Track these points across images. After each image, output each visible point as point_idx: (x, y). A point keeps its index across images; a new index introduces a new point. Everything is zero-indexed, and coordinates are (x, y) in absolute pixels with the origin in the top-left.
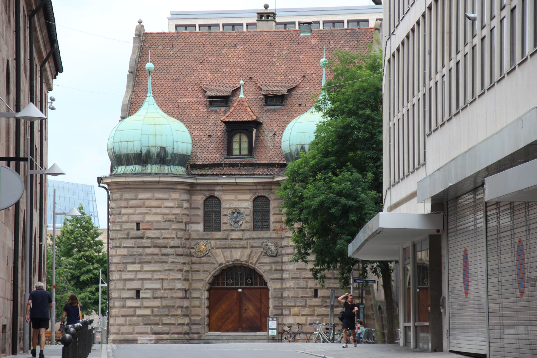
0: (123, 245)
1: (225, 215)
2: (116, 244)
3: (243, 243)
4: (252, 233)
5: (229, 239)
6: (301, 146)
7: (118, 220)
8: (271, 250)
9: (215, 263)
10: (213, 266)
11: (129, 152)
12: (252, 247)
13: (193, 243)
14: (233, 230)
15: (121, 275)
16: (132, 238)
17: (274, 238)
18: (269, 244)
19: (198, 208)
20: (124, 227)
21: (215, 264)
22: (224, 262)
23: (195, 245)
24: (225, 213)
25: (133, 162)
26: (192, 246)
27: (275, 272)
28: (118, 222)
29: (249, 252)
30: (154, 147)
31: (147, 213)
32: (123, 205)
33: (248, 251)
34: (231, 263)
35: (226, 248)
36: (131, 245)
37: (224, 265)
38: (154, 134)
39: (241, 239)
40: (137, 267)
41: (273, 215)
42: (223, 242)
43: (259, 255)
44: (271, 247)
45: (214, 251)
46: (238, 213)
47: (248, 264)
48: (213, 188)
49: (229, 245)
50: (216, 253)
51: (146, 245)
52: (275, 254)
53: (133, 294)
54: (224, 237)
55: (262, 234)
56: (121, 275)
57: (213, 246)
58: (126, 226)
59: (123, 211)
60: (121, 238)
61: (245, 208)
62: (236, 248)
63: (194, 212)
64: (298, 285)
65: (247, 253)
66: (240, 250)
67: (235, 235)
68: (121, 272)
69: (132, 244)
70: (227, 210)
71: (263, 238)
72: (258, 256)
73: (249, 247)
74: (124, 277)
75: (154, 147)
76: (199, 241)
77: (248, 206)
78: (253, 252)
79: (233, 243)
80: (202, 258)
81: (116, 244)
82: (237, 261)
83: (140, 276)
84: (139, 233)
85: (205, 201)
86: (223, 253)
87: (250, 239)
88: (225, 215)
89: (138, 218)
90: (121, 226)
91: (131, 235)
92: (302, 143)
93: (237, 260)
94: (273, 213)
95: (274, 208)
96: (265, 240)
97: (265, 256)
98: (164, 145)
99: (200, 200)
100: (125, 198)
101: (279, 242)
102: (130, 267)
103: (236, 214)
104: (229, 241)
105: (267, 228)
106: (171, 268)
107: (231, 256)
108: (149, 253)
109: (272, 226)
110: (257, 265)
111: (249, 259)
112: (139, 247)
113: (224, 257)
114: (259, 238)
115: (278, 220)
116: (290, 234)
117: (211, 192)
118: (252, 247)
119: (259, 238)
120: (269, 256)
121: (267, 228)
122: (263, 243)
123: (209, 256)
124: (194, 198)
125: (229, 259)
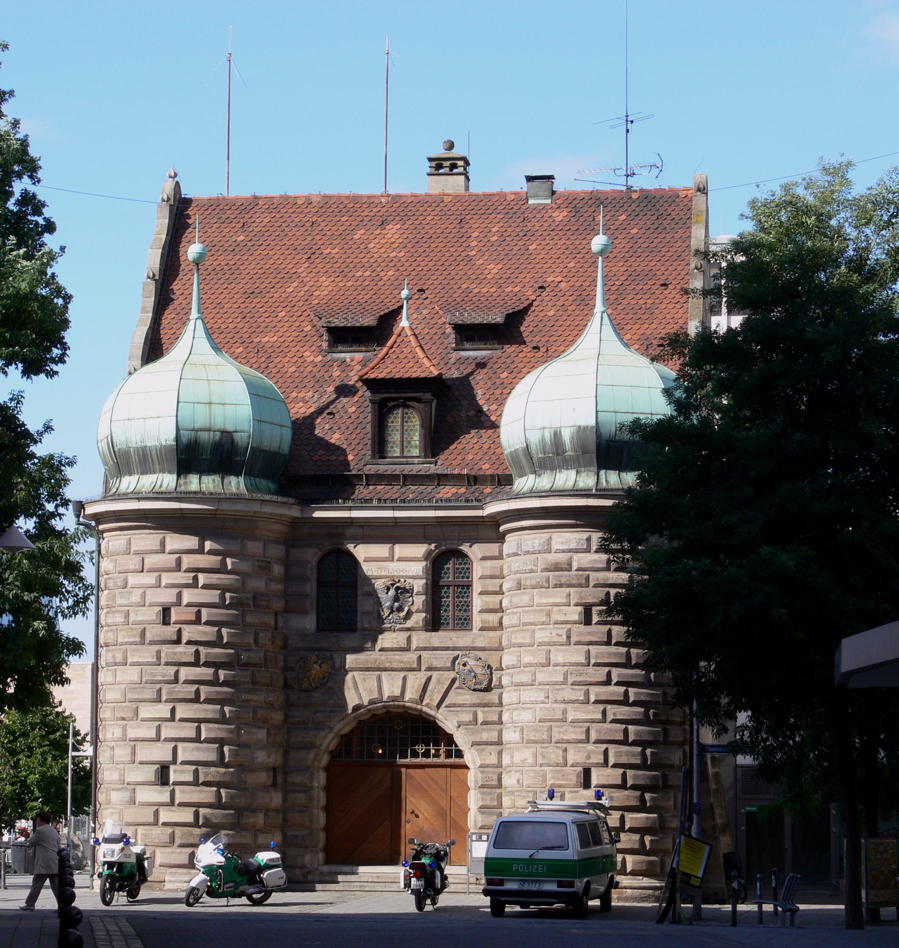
2: (114, 656)
4: (431, 637)
15: (124, 729)
16: (152, 643)
18: (472, 662)
25: (157, 467)
27: (484, 727)
29: (424, 681)
31: (187, 586)
33: (422, 676)
35: (368, 669)
36: (149, 660)
38: (208, 401)
40: (163, 710)
46: (397, 589)
49: (375, 662)
52: (483, 686)
53: (150, 773)
55: (454, 639)
56: (124, 729)
61: (414, 578)
62: (393, 670)
64: (544, 757)
68: (125, 722)
71: (454, 649)
73: (423, 668)
74: (132, 733)
75: (205, 430)
78: (433, 680)
81: (114, 656)
83: (168, 731)
84: (170, 631)
85: (320, 562)
96: (460, 653)
97: (460, 691)
98: (230, 428)
100: (137, 549)
102: (147, 711)
105: (464, 623)
109: (477, 620)
110: (441, 710)
112: (167, 664)
114: (447, 649)
116: (523, 638)
118: (430, 669)
119: (447, 649)
121: (464, 623)
122: (456, 659)
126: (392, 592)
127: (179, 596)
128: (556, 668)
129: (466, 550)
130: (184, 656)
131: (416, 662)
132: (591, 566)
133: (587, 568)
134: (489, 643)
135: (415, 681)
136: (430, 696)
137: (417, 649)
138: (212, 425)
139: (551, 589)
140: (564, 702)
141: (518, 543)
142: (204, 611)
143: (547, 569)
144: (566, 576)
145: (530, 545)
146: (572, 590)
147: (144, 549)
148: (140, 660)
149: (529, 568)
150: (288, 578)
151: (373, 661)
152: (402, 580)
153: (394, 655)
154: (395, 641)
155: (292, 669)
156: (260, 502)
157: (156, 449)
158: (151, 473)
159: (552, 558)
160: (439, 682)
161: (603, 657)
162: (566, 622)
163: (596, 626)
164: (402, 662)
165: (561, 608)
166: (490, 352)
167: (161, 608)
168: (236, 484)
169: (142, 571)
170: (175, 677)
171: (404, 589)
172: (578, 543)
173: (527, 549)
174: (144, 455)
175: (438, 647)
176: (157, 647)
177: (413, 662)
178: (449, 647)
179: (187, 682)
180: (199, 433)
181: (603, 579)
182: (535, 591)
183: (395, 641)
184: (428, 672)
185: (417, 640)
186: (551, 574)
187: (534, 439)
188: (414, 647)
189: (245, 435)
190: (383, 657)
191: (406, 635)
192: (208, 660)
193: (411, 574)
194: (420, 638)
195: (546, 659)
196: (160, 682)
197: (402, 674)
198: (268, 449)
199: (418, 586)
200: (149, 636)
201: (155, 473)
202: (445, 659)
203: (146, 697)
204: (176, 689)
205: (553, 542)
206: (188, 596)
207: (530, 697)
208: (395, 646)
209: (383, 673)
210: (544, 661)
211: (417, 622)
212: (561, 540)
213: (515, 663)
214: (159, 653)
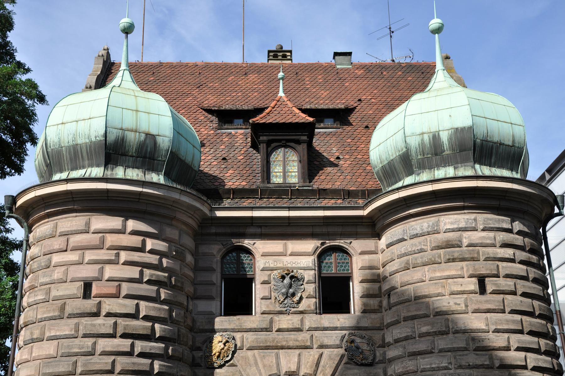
0: (47, 334)
2: (32, 333)
3: (304, 337)
4: (321, 318)
5: (275, 329)
6: (431, 135)
7: (42, 280)
8: (362, 353)
11: (79, 141)
12: (321, 347)
14: (281, 313)
16: (71, 316)
20: (54, 293)
25: (86, 162)
28: (42, 284)
29: (317, 357)
30: (132, 131)
31: (109, 262)
32: (56, 247)
33: (314, 354)
35: (267, 348)
36: (67, 333)
38: (135, 109)
42: (263, 336)
44: (360, 345)
46: (292, 277)
48: (242, 230)
49: (273, 341)
51: (103, 331)
54: (264, 326)
55: (341, 320)
58: (57, 291)
59: (56, 258)
60: (45, 319)
61: (305, 269)
62: (289, 348)
63: (203, 277)
67: (285, 321)
69: (71, 331)
73: (315, 346)
75: (132, 131)
78: (324, 356)
79: (282, 338)
81: (32, 333)
84: (89, 305)
87: (316, 329)
89: (88, 272)
90: (49, 292)
91: (68, 310)
92: (434, 129)
98: (154, 131)
99: (215, 253)
100: (63, 230)
101: (377, 336)
103: (287, 280)
104: (274, 335)
108: (108, 349)
112: (85, 336)
114: (335, 329)
118: (321, 347)
119: (335, 329)
120: (357, 364)
124: (204, 249)
126: (287, 280)
127: (101, 271)
128: (456, 335)
129: (347, 247)
130: (103, 327)
131: (309, 340)
132: (480, 242)
133: (477, 244)
134: (372, 323)
135: (310, 356)
136: (322, 370)
137: (310, 330)
138: (138, 127)
139: (443, 265)
140: (469, 367)
141: (404, 230)
142: (124, 285)
143: (438, 246)
144: (458, 251)
145: (419, 229)
146: (464, 264)
147: (69, 229)
148: (58, 334)
150: (196, 269)
152: (295, 271)
153: (290, 335)
154: (290, 322)
156: (180, 191)
157: (87, 148)
158: (80, 169)
159: (442, 237)
160: (330, 358)
161: (502, 324)
162: (463, 293)
163: (491, 295)
164: (297, 341)
165: (455, 280)
166: (335, 129)
167: (82, 283)
168: (157, 178)
169: (66, 251)
170: (93, 349)
171: (296, 277)
172: (466, 223)
173: (415, 232)
174: (75, 153)
175: (328, 328)
176: (76, 320)
177: (307, 341)
178: (337, 327)
179: (105, 353)
180: (126, 132)
181: (493, 253)
182: (426, 268)
183: (290, 322)
184: (320, 350)
185: (310, 322)
186: (442, 251)
187: (414, 142)
188: (307, 328)
189: (167, 139)
190: (281, 337)
191: (299, 317)
192: (127, 331)
193: (302, 266)
194: (311, 320)
195: (446, 327)
196: (76, 354)
197: (297, 352)
198: (183, 159)
199: (309, 275)
200: (68, 310)
201: (84, 167)
202: (334, 338)
203: (60, 370)
204: (92, 361)
205: (442, 224)
206: (110, 272)
207: (431, 364)
208: (291, 327)
209: (281, 351)
210: (444, 329)
211: (309, 306)
212: (450, 221)
213: (409, 334)
214: (77, 326)
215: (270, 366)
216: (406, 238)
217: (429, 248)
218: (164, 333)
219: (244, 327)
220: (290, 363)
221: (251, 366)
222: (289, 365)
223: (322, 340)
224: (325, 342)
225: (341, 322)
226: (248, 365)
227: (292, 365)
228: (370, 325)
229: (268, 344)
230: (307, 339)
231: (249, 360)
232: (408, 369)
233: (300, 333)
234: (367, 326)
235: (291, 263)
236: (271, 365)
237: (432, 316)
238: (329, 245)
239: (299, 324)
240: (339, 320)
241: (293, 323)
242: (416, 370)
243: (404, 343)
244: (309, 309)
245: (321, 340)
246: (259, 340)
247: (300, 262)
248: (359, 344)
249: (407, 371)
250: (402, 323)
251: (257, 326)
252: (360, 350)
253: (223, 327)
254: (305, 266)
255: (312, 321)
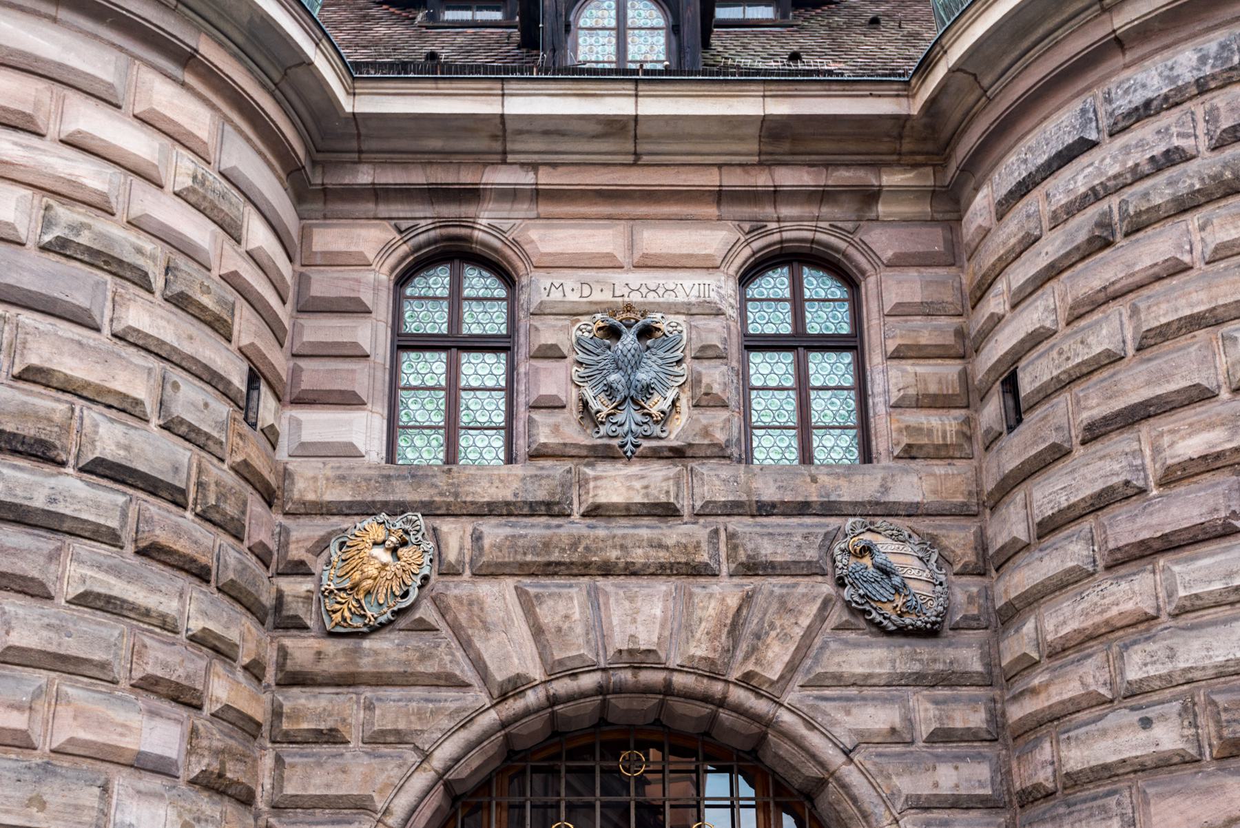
1: (551, 353)
5: (577, 510)
9: (465, 671)
10: (450, 698)
12: (752, 568)
13: (304, 532)
17: (913, 511)
18: (886, 547)
19: (355, 308)
21: (464, 685)
22: (537, 674)
23: (321, 546)
24: (547, 337)
26: (296, 552)
29: (733, 602)
34: (588, 681)
37: (532, 698)
39: (666, 512)
41: (898, 355)
42: (535, 530)
43: (805, 622)
44: (895, 561)
45: (460, 589)
47: (718, 688)
48: (467, 177)
49: (574, 545)
50: (472, 602)
54: (541, 495)
57: (451, 555)
61: (688, 310)
62: (632, 571)
65: (712, 609)
66: (662, 586)
70: (566, 321)
71: (830, 509)
72: (798, 632)
76: (346, 523)
77: (714, 296)
78: (760, 599)
80: (366, 644)
82: (636, 668)
86: (528, 604)
88: (551, 353)
93: (638, 659)
94: (891, 346)
95: (901, 311)
99: (371, 256)
104: (576, 527)
106: (72, 647)
107: (598, 628)
111: (730, 651)
113: (538, 631)
114: (802, 509)
115: (933, 389)
117: (450, 211)
118: (752, 568)
119: (802, 509)
123: (423, 627)
124: (328, 239)
125: (577, 647)
129: (842, 245)
149: (1158, 150)
151: (566, 541)
153: (635, 527)
154: (637, 485)
155: (299, 569)
164: (660, 546)
175: (773, 505)
177: (697, 546)
183: (637, 485)
184: (745, 581)
190: (601, 533)
193: (682, 298)
202: (798, 539)
208: (638, 499)
213: (1115, 480)
215: (559, 630)
216: (1093, 136)
217: (1203, 143)
218: (122, 453)
219: (469, 499)
220: (634, 621)
221: (488, 630)
222: (631, 630)
223: (753, 546)
224: (763, 552)
225: (823, 486)
226: (480, 625)
227: (641, 628)
228: (931, 498)
229: (555, 556)
230: (698, 543)
231: (482, 609)
232: (1114, 611)
233: (672, 521)
234: (918, 499)
235: (644, 290)
236: (565, 626)
237: (1225, 394)
238: (776, 237)
239: (668, 492)
240: (814, 480)
241: (646, 487)
242: (1152, 612)
243: (1088, 524)
244: (706, 442)
245: (750, 546)
246: (521, 542)
247: (672, 287)
248: (891, 558)
249: (1107, 622)
250: (1079, 451)
251: (516, 495)
252: (896, 580)
253: (391, 498)
254: (693, 300)
255: (717, 483)
